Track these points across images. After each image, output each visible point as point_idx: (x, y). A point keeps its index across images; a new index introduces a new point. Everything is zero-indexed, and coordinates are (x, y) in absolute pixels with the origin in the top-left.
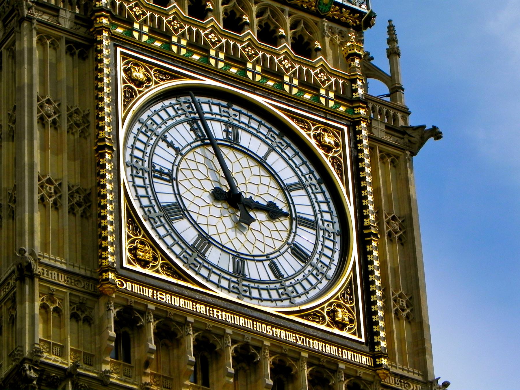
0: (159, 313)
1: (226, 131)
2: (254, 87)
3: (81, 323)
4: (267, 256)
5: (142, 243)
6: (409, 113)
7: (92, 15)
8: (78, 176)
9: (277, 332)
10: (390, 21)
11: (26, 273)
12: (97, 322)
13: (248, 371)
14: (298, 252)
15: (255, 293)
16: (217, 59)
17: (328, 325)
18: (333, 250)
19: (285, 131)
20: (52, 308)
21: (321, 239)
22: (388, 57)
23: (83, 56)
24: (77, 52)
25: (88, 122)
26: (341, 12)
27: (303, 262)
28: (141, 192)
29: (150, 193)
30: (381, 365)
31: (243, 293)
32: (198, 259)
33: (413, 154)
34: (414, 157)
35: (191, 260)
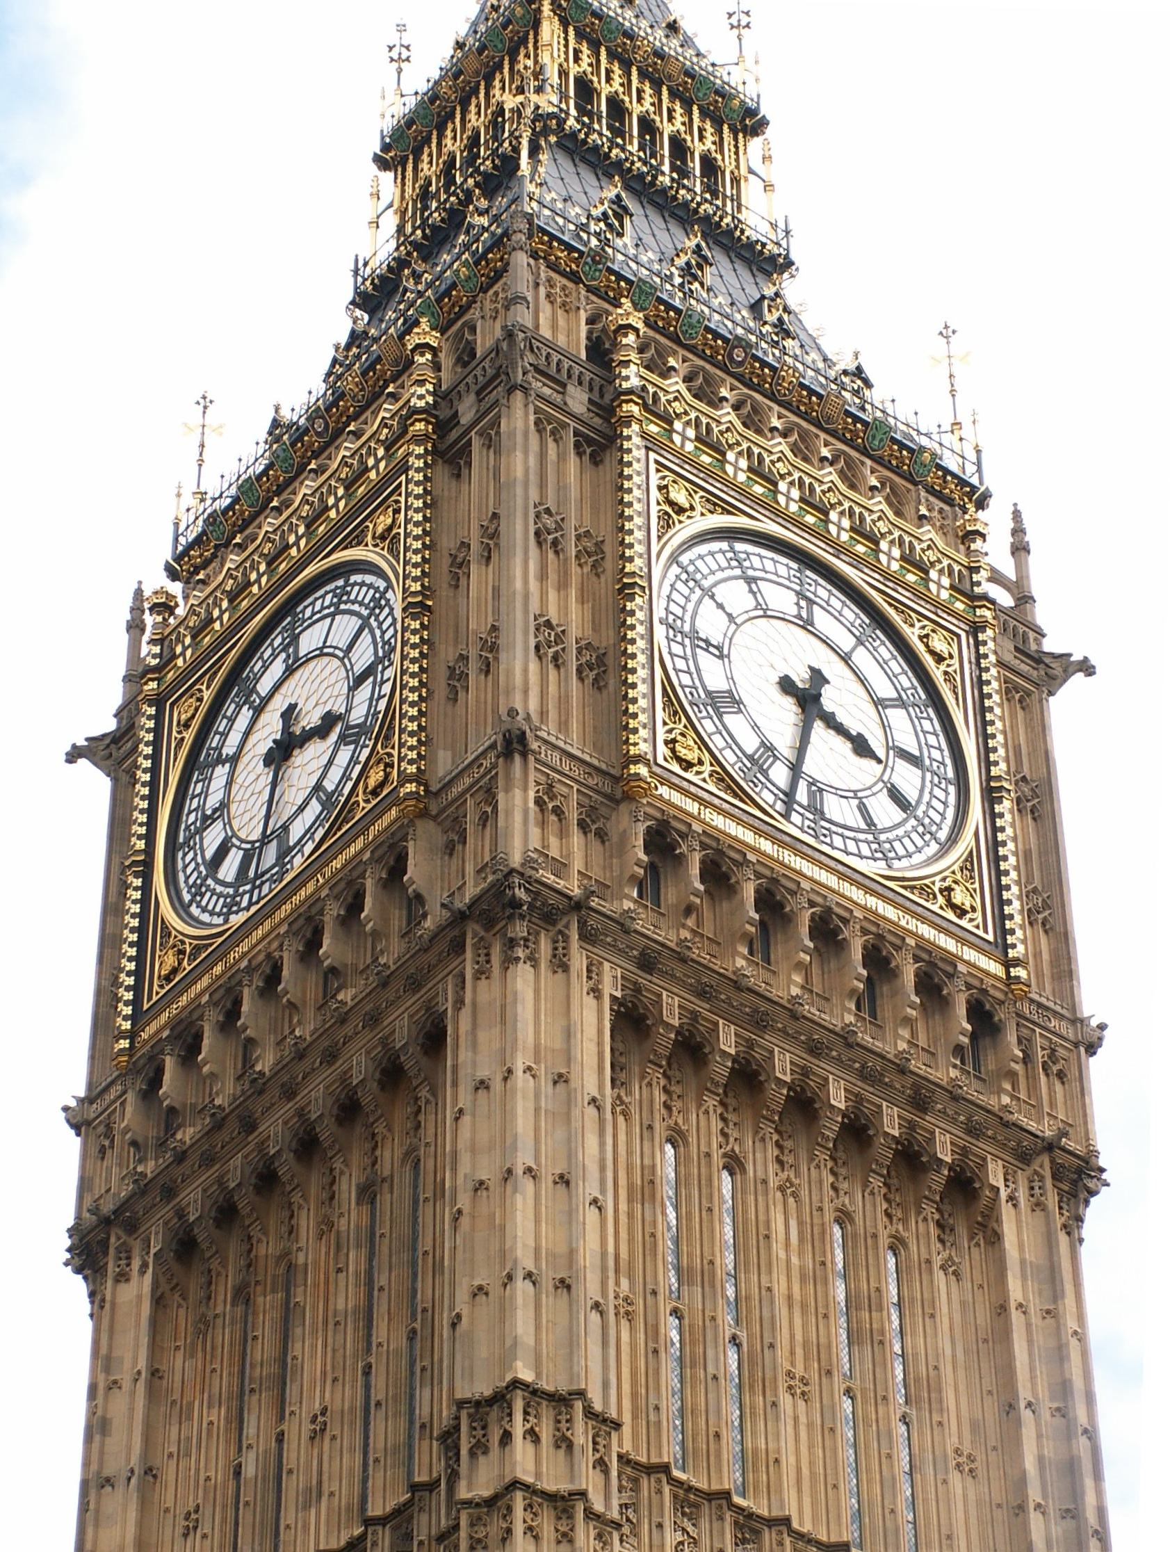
0: (708, 841)
1: (797, 604)
2: (840, 550)
3: (591, 836)
4: (855, 792)
5: (683, 735)
6: (1044, 636)
7: (613, 400)
8: (588, 626)
9: (872, 902)
10: (1015, 505)
11: (515, 745)
12: (615, 839)
13: (825, 955)
14: (896, 796)
15: (838, 842)
17: (941, 908)
18: (945, 804)
20: (550, 806)
21: (928, 784)
22: (1013, 553)
23: (596, 461)
24: (588, 451)
25: (603, 552)
26: (945, 482)
27: (904, 811)
28: (681, 664)
29: (693, 669)
31: (822, 838)
32: (759, 775)
33: (1051, 693)
34: (1051, 699)
35: (750, 776)
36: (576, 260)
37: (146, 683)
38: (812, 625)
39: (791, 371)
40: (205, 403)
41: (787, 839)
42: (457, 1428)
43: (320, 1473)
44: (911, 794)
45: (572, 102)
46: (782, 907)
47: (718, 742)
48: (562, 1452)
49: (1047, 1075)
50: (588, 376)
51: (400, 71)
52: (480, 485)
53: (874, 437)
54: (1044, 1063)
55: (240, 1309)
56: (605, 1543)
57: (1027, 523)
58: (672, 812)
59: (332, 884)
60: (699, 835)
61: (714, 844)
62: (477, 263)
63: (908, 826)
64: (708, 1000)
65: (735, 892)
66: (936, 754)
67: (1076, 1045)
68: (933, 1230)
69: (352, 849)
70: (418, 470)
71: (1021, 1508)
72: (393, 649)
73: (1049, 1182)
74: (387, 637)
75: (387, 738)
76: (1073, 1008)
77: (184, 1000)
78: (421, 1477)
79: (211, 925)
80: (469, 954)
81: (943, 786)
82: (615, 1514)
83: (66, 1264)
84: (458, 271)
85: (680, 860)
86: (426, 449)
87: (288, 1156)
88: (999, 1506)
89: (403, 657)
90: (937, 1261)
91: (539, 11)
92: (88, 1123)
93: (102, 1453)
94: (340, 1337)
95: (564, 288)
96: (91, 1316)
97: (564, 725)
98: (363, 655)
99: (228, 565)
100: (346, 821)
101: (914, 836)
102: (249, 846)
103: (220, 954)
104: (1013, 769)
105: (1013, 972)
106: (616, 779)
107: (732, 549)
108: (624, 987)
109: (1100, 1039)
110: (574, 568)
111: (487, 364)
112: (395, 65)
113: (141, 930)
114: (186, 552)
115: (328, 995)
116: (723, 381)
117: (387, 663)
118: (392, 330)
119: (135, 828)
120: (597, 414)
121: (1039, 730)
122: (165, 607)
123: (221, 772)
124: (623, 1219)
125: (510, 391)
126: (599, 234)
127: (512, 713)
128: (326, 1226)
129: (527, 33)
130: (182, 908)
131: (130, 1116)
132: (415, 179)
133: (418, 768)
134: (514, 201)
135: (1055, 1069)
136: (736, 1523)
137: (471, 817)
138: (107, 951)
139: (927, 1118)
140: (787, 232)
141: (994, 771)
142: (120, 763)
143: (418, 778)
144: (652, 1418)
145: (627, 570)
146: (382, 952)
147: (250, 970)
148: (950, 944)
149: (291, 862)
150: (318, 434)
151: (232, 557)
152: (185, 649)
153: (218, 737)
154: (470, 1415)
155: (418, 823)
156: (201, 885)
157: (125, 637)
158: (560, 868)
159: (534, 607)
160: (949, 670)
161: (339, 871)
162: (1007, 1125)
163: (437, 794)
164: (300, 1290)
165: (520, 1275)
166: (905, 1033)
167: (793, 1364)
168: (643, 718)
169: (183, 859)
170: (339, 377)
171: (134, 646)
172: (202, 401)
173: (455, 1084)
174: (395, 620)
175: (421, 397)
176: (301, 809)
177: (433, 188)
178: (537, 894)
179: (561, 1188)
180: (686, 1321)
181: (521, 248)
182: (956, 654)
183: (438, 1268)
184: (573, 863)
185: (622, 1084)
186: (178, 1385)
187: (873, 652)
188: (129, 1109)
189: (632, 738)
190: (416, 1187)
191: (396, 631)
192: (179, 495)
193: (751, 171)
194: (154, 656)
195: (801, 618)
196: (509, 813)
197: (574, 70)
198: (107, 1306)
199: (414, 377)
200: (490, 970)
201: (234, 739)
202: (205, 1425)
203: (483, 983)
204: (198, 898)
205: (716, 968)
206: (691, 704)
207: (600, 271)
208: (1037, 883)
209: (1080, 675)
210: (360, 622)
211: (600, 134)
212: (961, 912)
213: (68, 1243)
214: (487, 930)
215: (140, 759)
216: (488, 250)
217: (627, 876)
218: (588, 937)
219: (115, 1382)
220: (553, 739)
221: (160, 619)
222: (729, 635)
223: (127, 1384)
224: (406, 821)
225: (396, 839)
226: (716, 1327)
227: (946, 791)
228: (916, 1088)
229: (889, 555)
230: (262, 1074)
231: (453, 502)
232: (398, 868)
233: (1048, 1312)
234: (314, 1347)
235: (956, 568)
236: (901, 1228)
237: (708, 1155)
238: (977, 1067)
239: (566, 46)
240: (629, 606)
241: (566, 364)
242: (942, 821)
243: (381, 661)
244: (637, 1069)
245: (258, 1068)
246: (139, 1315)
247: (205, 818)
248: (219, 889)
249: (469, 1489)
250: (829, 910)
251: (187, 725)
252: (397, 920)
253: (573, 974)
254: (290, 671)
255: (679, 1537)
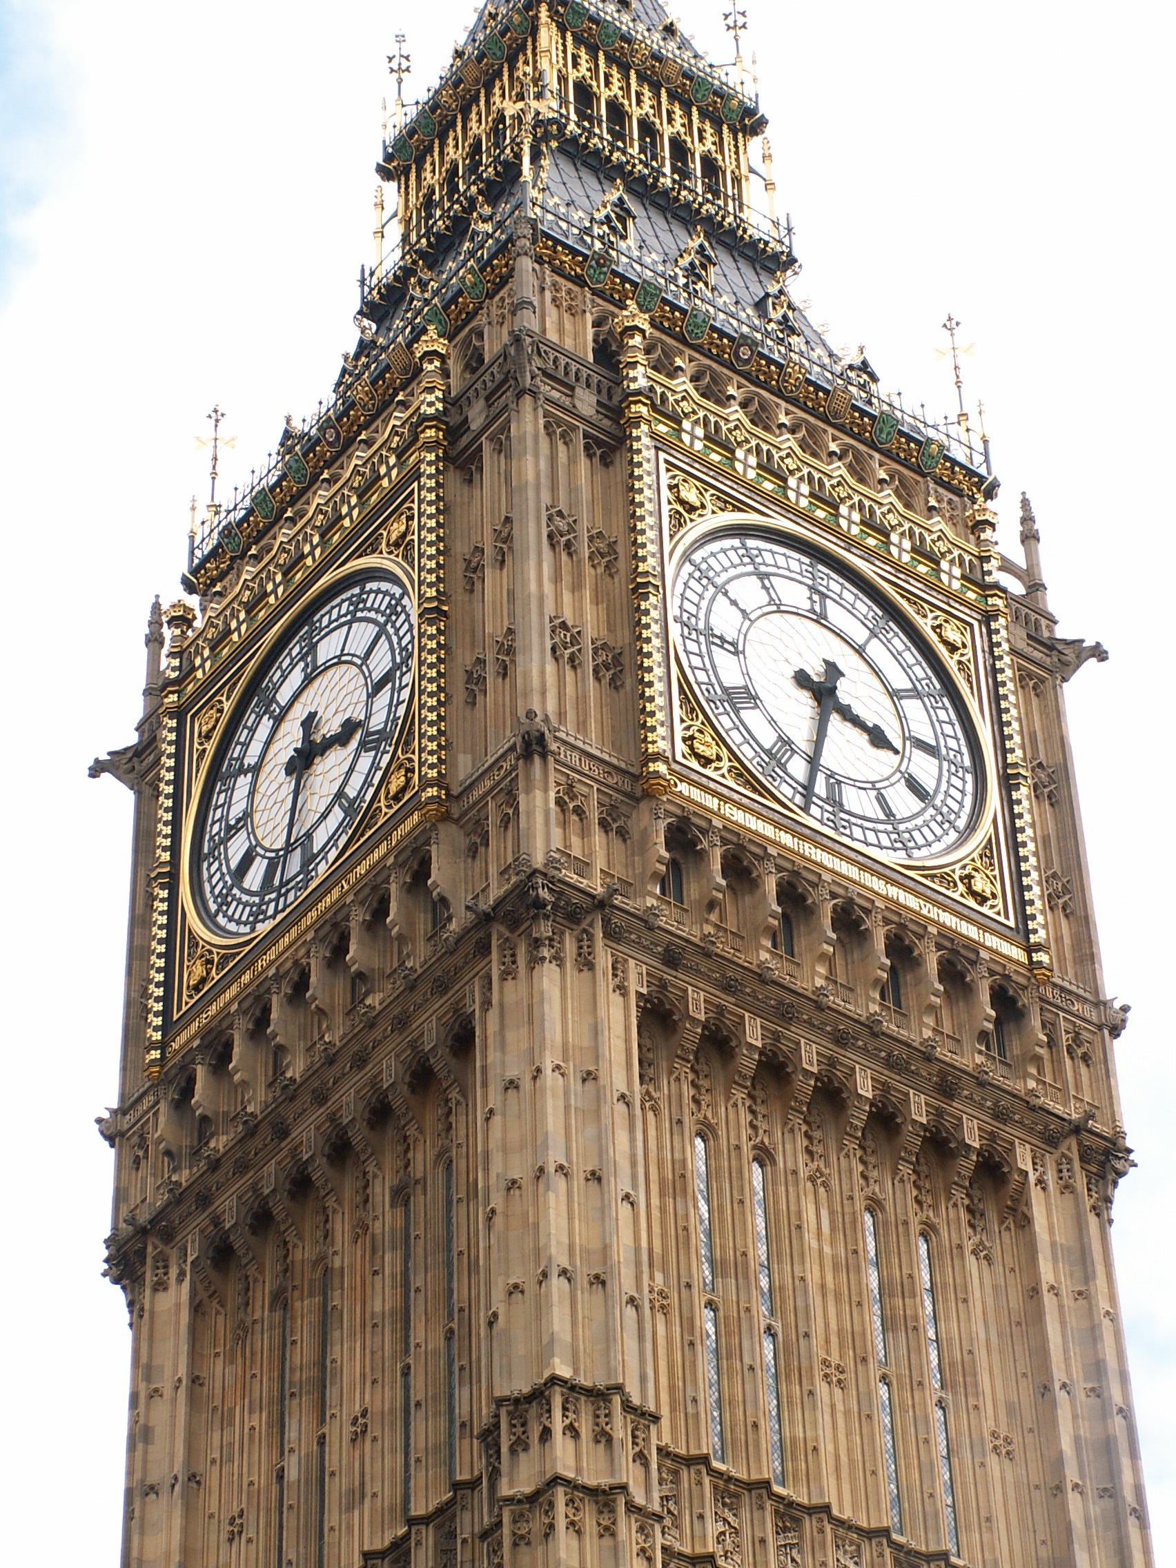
0: (728, 836)
1: (810, 598)
2: (851, 543)
3: (612, 834)
4: (873, 783)
5: (700, 731)
6: (1055, 623)
7: (621, 402)
9: (893, 891)
10: (1024, 493)
12: (636, 836)
13: (848, 946)
14: (914, 786)
15: (857, 833)
16: (799, 493)
17: (962, 895)
18: (963, 792)
19: (892, 612)
20: (571, 806)
21: (945, 773)
22: (1023, 542)
23: (606, 462)
24: (598, 453)
26: (953, 472)
28: (696, 661)
29: (708, 666)
30: (1040, 962)
31: (842, 830)
32: (777, 769)
33: (1064, 680)
34: (1065, 685)
35: (768, 770)
36: (580, 264)
37: (166, 696)
38: (825, 618)
39: (797, 368)
40: (217, 416)
41: (807, 832)
42: (497, 1426)
43: (362, 1475)
44: (929, 784)
45: (572, 107)
46: (804, 899)
47: (735, 738)
48: (601, 1447)
49: (1072, 1058)
50: (595, 378)
51: (400, 81)
52: (492, 490)
53: (881, 431)
54: (1069, 1047)
55: (278, 1315)
56: (647, 1536)
57: (1036, 512)
58: (692, 808)
59: (357, 890)
60: (719, 830)
61: (735, 839)
62: (482, 270)
63: (927, 816)
64: (733, 994)
65: (757, 886)
66: (952, 743)
67: (1100, 1027)
68: (964, 1216)
69: (376, 855)
70: (430, 477)
71: (1059, 1489)
72: (411, 655)
73: (1077, 1164)
74: (404, 643)
75: (407, 743)
76: (1096, 991)
77: (213, 1009)
78: (463, 1476)
79: (237, 934)
80: (495, 955)
81: (960, 774)
82: (656, 1507)
83: (104, 1275)
84: (464, 278)
85: (701, 856)
86: (437, 456)
87: (321, 1161)
88: (1037, 1487)
89: (421, 663)
90: (968, 1246)
91: (537, 17)
92: (122, 1134)
93: (145, 1461)
94: (378, 1339)
95: (569, 292)
96: (131, 1325)
97: (582, 726)
98: (381, 662)
99: (245, 576)
100: (369, 827)
101: (933, 825)
102: (273, 855)
103: (248, 962)
104: (1029, 756)
105: (1035, 957)
106: (636, 778)
107: (744, 545)
108: (649, 984)
109: (1124, 1021)
110: (588, 569)
111: (495, 369)
112: (395, 75)
113: (169, 941)
114: (202, 565)
115: (356, 1000)
116: (730, 379)
117: (404, 669)
118: (400, 339)
119: (159, 840)
120: (606, 416)
121: (1054, 716)
122: (183, 620)
123: (244, 782)
124: (656, 1213)
125: (519, 395)
126: (603, 237)
127: (531, 715)
128: (361, 1229)
129: (526, 40)
130: (209, 919)
131: (163, 1126)
132: (419, 188)
133: (439, 772)
134: (517, 207)
135: (1080, 1052)
136: (777, 1512)
137: (493, 821)
138: (136, 964)
139: (954, 1104)
140: (789, 230)
141: (1011, 758)
142: (143, 776)
143: (439, 782)
144: (690, 1410)
145: (640, 570)
146: (408, 956)
147: (278, 977)
148: (972, 932)
149: (315, 869)
150: (330, 444)
151: (248, 568)
152: (204, 661)
153: (239, 747)
154: (509, 1413)
155: (441, 826)
156: (227, 895)
157: (143, 652)
158: (583, 867)
159: (549, 609)
160: (963, 659)
161: (363, 876)
162: (1033, 1109)
163: (458, 797)
164: (337, 1293)
165: (555, 1272)
166: (930, 1020)
167: (828, 1352)
168: (660, 716)
169: (208, 869)
170: (349, 387)
171: (154, 660)
172: (213, 415)
173: (485, 1084)
174: (411, 626)
175: (431, 404)
176: (324, 816)
177: (437, 197)
178: (561, 893)
179: (593, 1185)
180: (721, 1313)
181: (526, 254)
182: (969, 644)
183: (473, 1267)
184: (595, 862)
185: (651, 1079)
186: (218, 1391)
187: (887, 644)
188: (162, 1119)
189: (651, 737)
190: (449, 1188)
191: (413, 637)
192: (193, 509)
193: (751, 171)
194: (174, 669)
195: (814, 612)
196: (529, 814)
197: (573, 75)
198: (146, 1315)
199: (424, 384)
200: (516, 971)
201: (255, 749)
202: (246, 1431)
203: (510, 984)
204: (225, 908)
205: (740, 962)
206: (708, 700)
207: (605, 274)
208: (1056, 868)
209: (1093, 660)
210: (377, 629)
211: (601, 138)
212: (982, 899)
213: (105, 1253)
214: (512, 931)
215: (163, 772)
216: (493, 256)
217: (649, 873)
218: (612, 935)
219: (156, 1390)
220: (571, 740)
221: (178, 632)
222: (744, 631)
223: (168, 1392)
224: (428, 825)
225: (419, 843)
226: (751, 1318)
227: (963, 779)
228: (943, 1075)
229: (899, 547)
230: (292, 1080)
231: (466, 507)
232: (422, 872)
233: (1080, 1293)
234: (352, 1350)
235: (967, 558)
236: (931, 1214)
237: (738, 1147)
238: (1002, 1053)
239: (565, 51)
240: (643, 605)
241: (574, 367)
242: (960, 810)
243: (399, 667)
244: (665, 1064)
245: (289, 1075)
246: (178, 1322)
247: (229, 828)
248: (245, 898)
249: (511, 1486)
250: (850, 901)
251: (208, 737)
252: (423, 924)
253: (599, 973)
254: (308, 680)
255: (721, 1527)
